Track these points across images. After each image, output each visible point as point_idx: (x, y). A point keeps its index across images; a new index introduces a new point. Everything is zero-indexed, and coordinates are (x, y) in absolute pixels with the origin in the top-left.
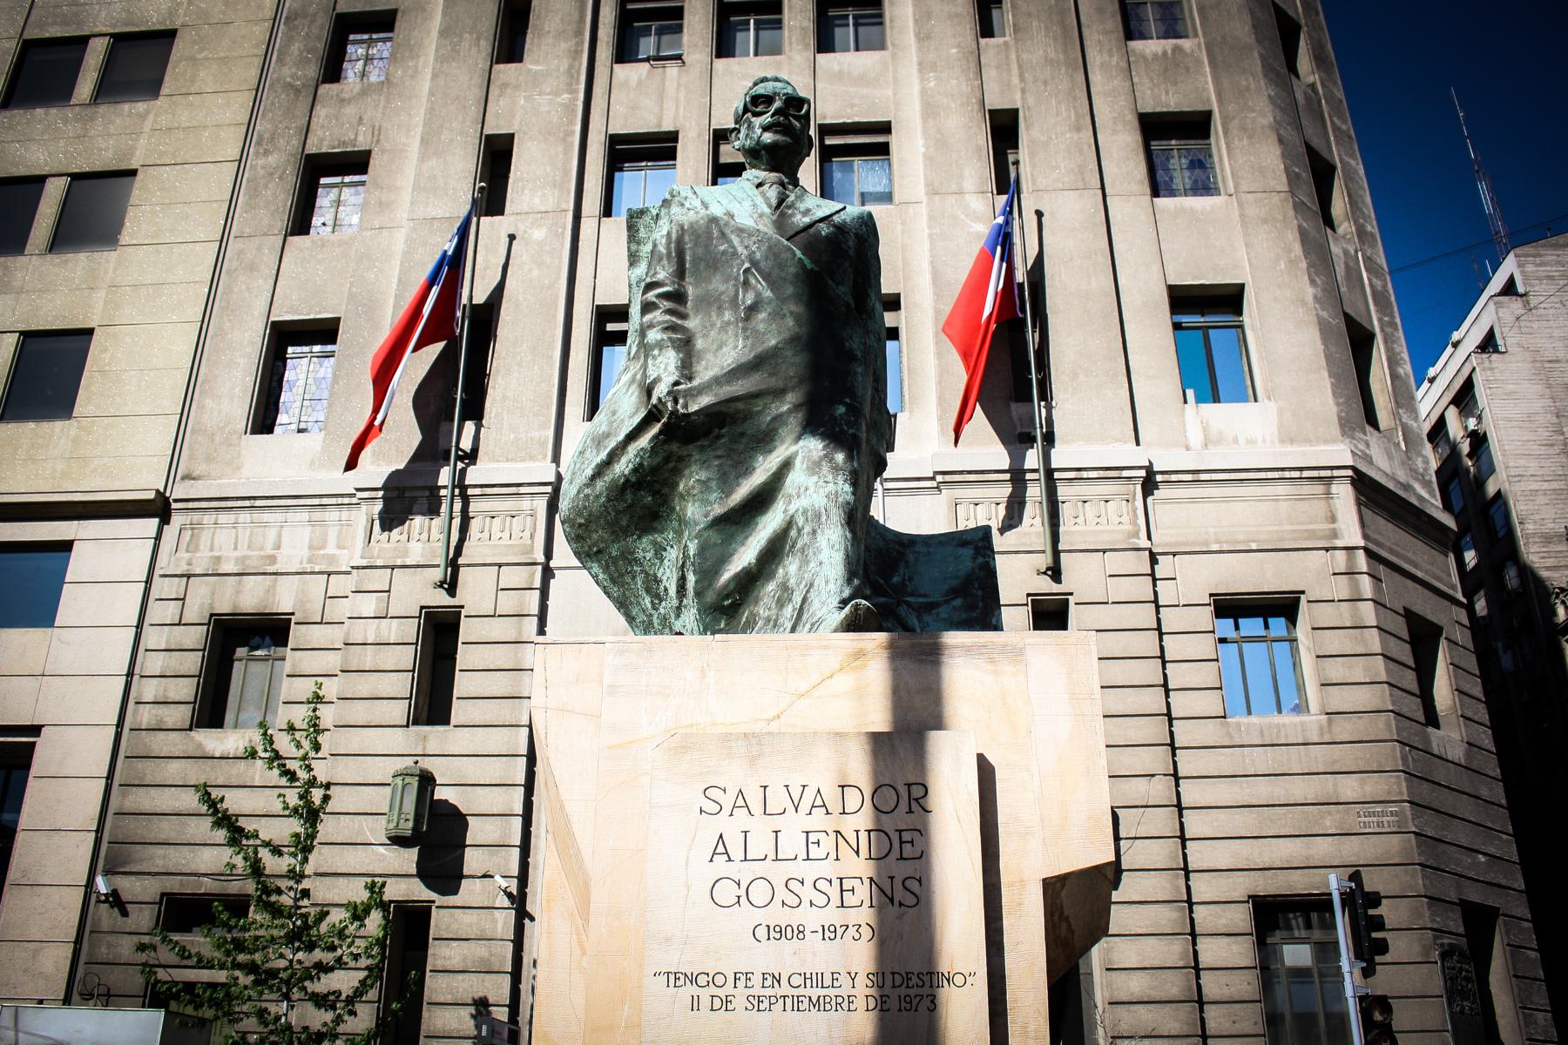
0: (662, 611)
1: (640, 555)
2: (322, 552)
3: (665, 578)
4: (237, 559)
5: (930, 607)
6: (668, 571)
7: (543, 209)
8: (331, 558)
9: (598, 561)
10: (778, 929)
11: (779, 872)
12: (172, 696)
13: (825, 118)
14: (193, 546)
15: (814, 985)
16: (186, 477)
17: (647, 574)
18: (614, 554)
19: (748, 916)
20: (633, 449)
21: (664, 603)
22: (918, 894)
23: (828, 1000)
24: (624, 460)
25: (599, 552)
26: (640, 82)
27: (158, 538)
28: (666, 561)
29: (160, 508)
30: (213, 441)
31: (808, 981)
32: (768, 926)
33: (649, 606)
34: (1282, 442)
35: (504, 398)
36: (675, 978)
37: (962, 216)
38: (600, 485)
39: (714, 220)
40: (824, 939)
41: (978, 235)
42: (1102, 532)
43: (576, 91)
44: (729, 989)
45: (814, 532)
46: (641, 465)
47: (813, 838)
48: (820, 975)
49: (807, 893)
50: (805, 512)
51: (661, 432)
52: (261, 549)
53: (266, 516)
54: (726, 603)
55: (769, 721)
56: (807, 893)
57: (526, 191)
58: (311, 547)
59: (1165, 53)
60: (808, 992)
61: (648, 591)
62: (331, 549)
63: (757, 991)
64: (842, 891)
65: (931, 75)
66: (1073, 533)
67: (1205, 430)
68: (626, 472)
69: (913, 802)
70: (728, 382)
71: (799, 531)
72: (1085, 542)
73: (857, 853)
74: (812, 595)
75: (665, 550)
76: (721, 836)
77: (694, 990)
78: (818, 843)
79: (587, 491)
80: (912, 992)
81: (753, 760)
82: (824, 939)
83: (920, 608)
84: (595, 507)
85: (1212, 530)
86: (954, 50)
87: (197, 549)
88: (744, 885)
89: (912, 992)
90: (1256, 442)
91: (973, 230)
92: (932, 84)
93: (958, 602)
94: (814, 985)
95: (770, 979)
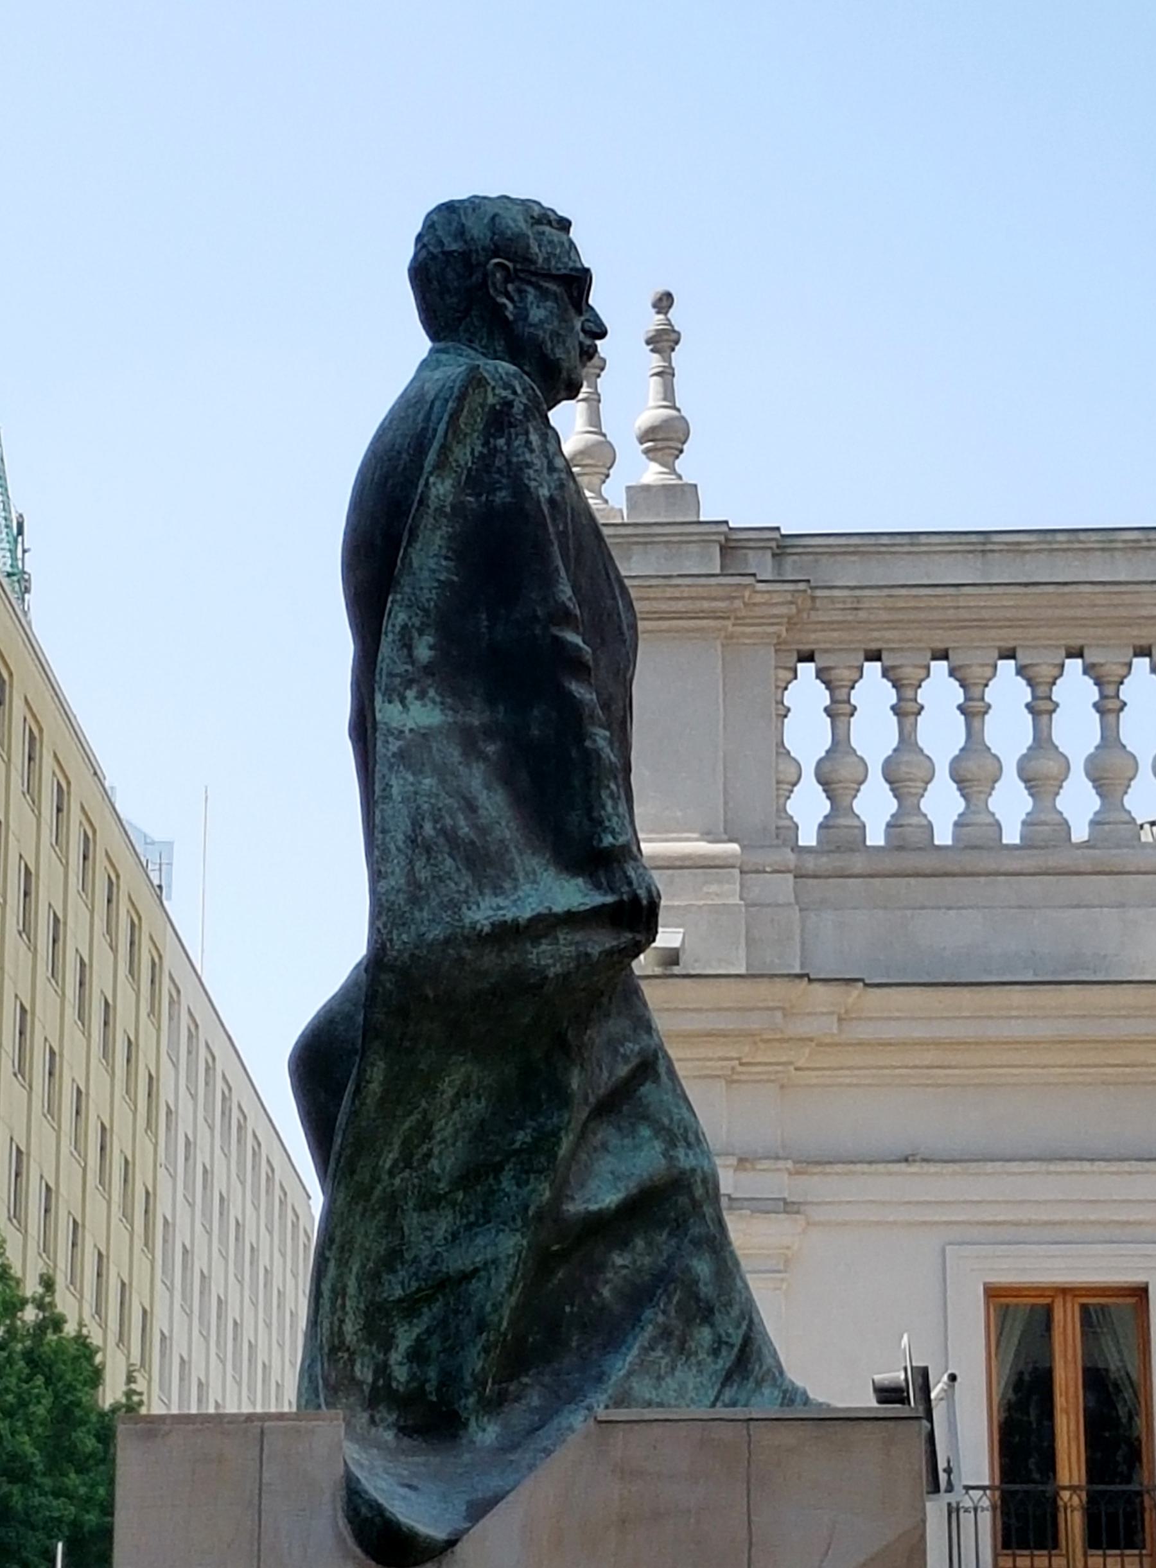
0: (397, 1181)
3: (438, 1138)
6: (450, 1130)
21: (406, 1174)
28: (456, 1114)
33: (388, 1165)
38: (489, 960)
61: (405, 1143)
68: (551, 972)
75: (467, 1096)
79: (467, 953)
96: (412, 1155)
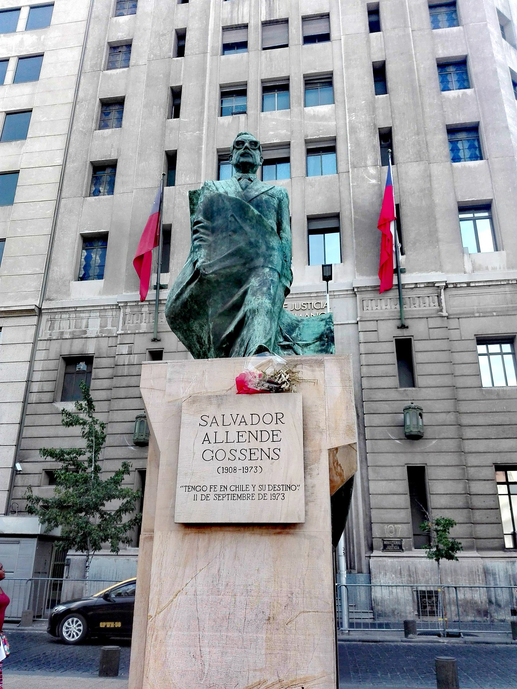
0: (204, 350)
1: (194, 328)
2: (105, 328)
3: (204, 337)
4: (70, 333)
5: (307, 345)
6: (205, 334)
7: (190, 183)
8: (110, 331)
9: (179, 331)
10: (226, 468)
11: (227, 447)
12: (45, 389)
13: (307, 136)
14: (51, 328)
15: (239, 490)
16: (49, 299)
17: (197, 336)
18: (185, 328)
19: (216, 464)
20: (189, 289)
22: (279, 454)
23: (244, 495)
24: (186, 292)
25: (180, 328)
26: (229, 124)
27: (38, 326)
28: (204, 331)
29: (39, 312)
30: (58, 284)
31: (237, 489)
32: (223, 468)
33: (199, 348)
34: (508, 268)
35: (178, 263)
36: (190, 488)
37: (366, 177)
39: (220, 195)
40: (243, 472)
41: (374, 185)
42: (427, 310)
43: (202, 130)
44: (208, 492)
45: (253, 318)
46: (192, 294)
47: (240, 434)
48: (241, 486)
49: (238, 455)
50: (250, 310)
51: (198, 281)
52: (80, 328)
53: (82, 315)
54: (224, 346)
55: (227, 391)
56: (238, 455)
57: (183, 175)
58: (101, 327)
59: (458, 96)
60: (237, 492)
61: (198, 342)
62: (109, 327)
63: (218, 492)
64: (251, 454)
65: (353, 114)
66: (413, 311)
67: (473, 263)
68: (187, 297)
69: (278, 420)
70: (224, 261)
71: (248, 318)
72: (419, 314)
73: (257, 439)
74: (250, 342)
75: (203, 326)
76: (207, 434)
77: (194, 492)
78: (242, 436)
80: (276, 492)
81: (219, 406)
82: (243, 472)
83: (303, 346)
84: (177, 311)
85: (475, 308)
86: (364, 102)
87: (53, 329)
88: (214, 452)
89: (276, 492)
90: (496, 269)
91: (371, 182)
92: (354, 118)
93: (318, 343)
94: (239, 490)
95: (223, 488)
96: (202, 343)
